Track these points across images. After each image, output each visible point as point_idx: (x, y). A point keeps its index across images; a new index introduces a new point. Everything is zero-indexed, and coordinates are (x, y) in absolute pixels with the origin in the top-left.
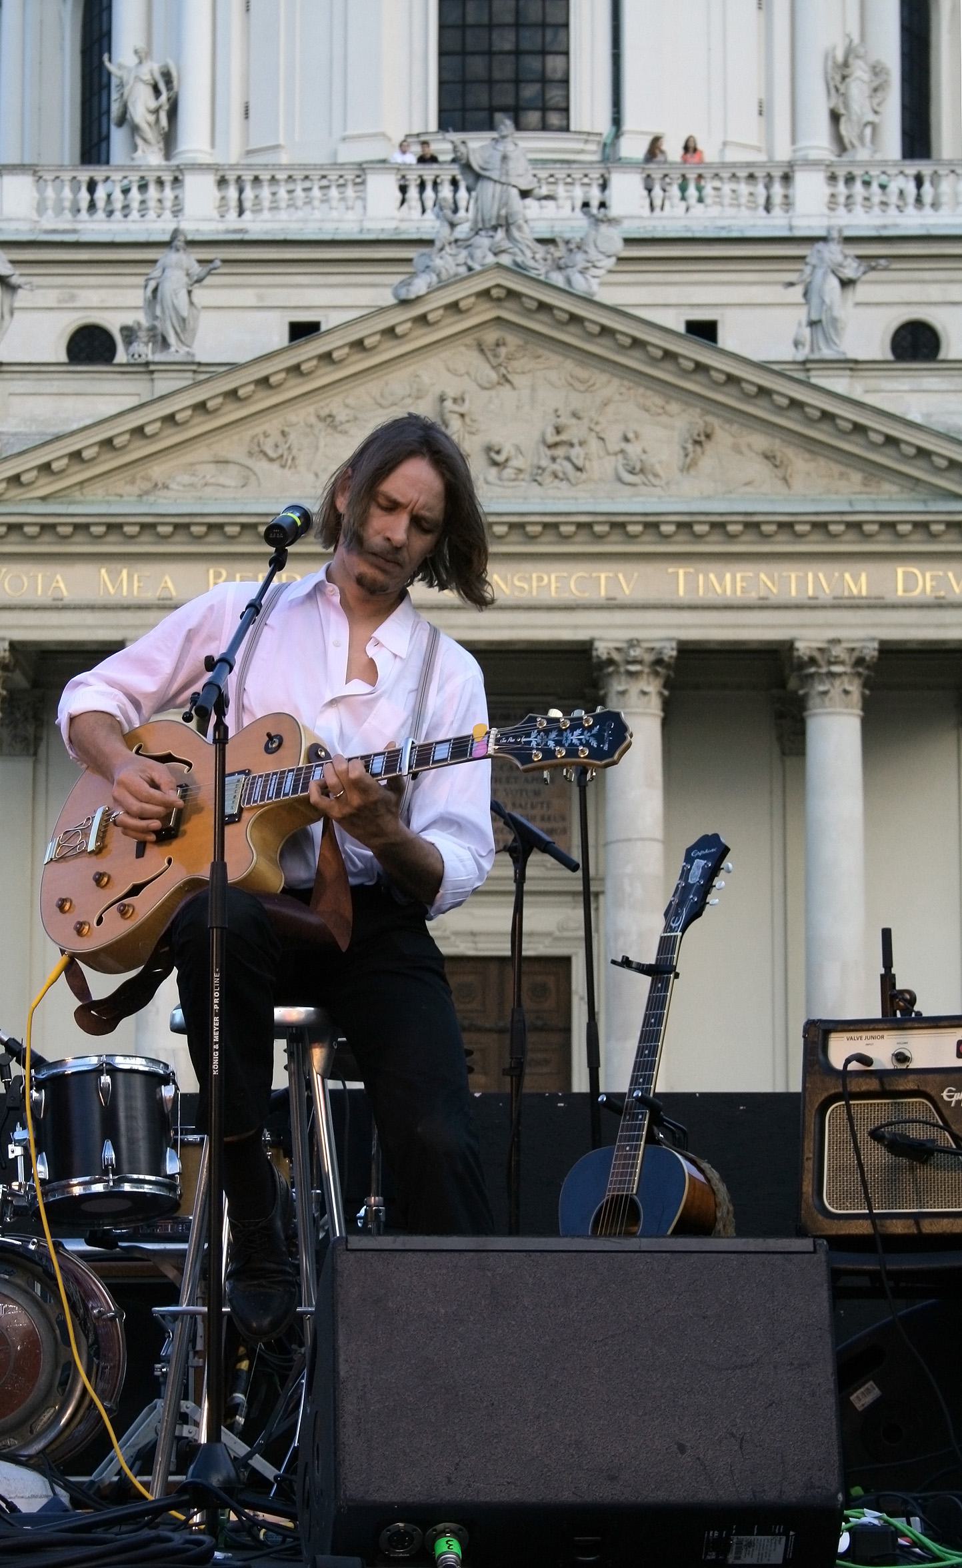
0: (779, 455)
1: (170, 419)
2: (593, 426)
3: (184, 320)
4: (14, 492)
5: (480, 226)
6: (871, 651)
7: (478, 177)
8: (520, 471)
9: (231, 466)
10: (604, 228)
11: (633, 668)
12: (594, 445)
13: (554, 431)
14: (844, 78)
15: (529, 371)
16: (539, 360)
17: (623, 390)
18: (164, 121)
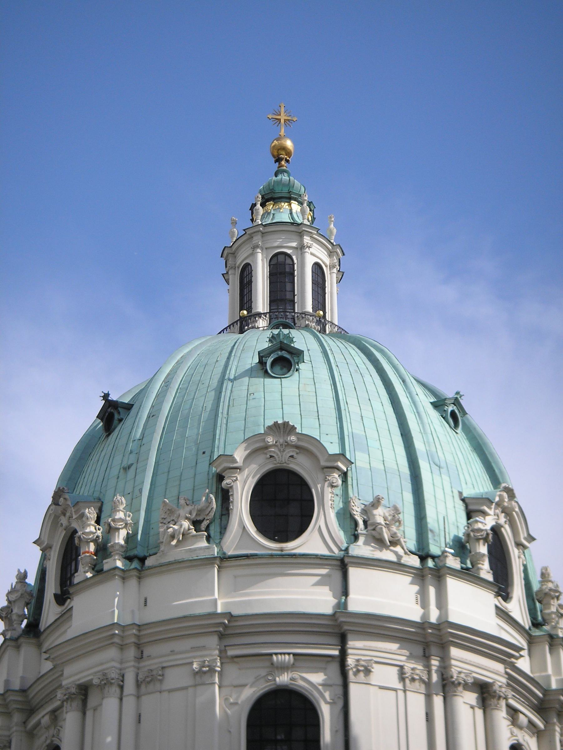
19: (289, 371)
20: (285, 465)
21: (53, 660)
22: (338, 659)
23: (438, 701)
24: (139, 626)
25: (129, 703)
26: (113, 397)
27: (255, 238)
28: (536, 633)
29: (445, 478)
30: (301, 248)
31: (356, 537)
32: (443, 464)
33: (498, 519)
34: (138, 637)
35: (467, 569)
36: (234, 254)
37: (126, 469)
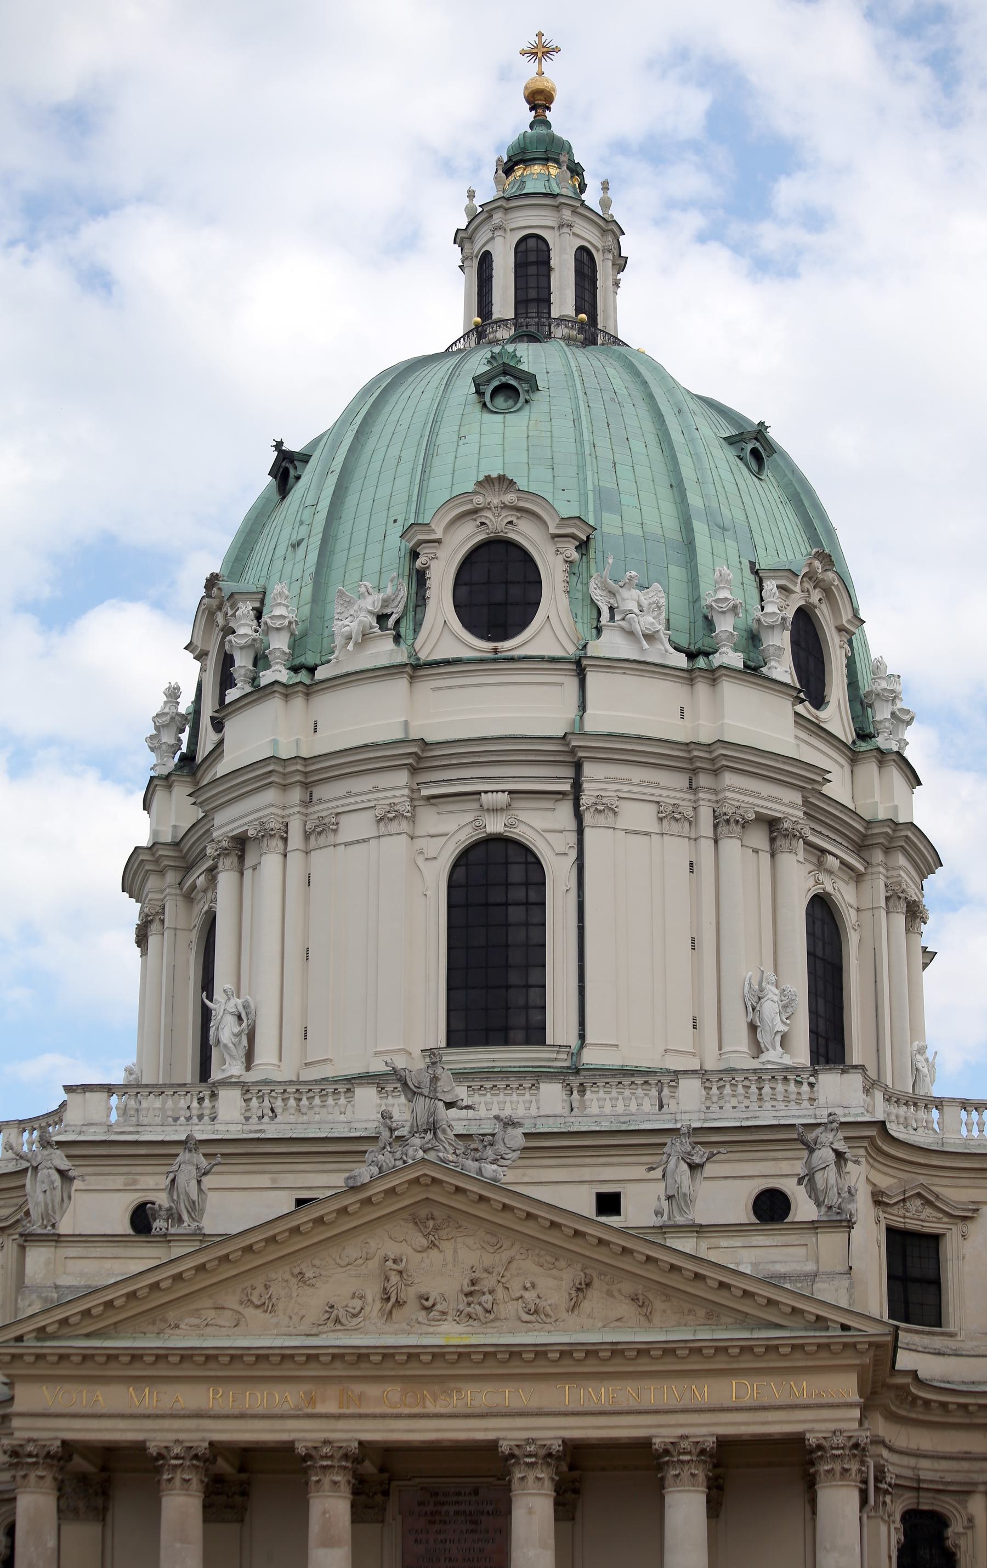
0: (641, 1297)
1: (178, 1277)
2: (499, 1278)
3: (194, 1202)
4: (65, 1331)
5: (415, 1130)
6: (710, 1442)
7: (415, 1093)
8: (444, 1313)
9: (226, 1312)
10: (510, 1130)
11: (528, 1460)
12: (500, 1291)
13: (470, 1283)
14: (760, 998)
15: (452, 1238)
16: (458, 1230)
17: (523, 1251)
18: (245, 1042)
19: (516, 403)
20: (501, 534)
21: (201, 804)
22: (571, 797)
23: (707, 846)
24: (305, 759)
25: (295, 859)
26: (288, 446)
27: (495, 217)
28: (863, 746)
29: (731, 543)
30: (561, 226)
31: (599, 630)
32: (727, 524)
33: (809, 597)
34: (306, 774)
35: (756, 669)
36: (471, 239)
37: (296, 545)
